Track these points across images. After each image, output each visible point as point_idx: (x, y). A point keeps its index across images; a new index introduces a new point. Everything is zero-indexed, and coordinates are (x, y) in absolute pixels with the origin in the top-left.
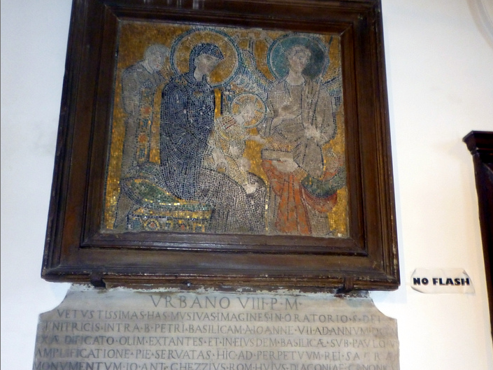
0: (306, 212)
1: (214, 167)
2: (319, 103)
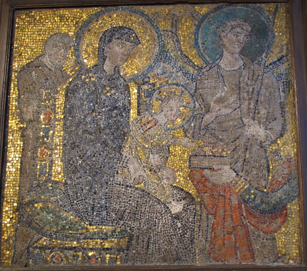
0: (247, 233)
1: (130, 182)
2: (263, 91)
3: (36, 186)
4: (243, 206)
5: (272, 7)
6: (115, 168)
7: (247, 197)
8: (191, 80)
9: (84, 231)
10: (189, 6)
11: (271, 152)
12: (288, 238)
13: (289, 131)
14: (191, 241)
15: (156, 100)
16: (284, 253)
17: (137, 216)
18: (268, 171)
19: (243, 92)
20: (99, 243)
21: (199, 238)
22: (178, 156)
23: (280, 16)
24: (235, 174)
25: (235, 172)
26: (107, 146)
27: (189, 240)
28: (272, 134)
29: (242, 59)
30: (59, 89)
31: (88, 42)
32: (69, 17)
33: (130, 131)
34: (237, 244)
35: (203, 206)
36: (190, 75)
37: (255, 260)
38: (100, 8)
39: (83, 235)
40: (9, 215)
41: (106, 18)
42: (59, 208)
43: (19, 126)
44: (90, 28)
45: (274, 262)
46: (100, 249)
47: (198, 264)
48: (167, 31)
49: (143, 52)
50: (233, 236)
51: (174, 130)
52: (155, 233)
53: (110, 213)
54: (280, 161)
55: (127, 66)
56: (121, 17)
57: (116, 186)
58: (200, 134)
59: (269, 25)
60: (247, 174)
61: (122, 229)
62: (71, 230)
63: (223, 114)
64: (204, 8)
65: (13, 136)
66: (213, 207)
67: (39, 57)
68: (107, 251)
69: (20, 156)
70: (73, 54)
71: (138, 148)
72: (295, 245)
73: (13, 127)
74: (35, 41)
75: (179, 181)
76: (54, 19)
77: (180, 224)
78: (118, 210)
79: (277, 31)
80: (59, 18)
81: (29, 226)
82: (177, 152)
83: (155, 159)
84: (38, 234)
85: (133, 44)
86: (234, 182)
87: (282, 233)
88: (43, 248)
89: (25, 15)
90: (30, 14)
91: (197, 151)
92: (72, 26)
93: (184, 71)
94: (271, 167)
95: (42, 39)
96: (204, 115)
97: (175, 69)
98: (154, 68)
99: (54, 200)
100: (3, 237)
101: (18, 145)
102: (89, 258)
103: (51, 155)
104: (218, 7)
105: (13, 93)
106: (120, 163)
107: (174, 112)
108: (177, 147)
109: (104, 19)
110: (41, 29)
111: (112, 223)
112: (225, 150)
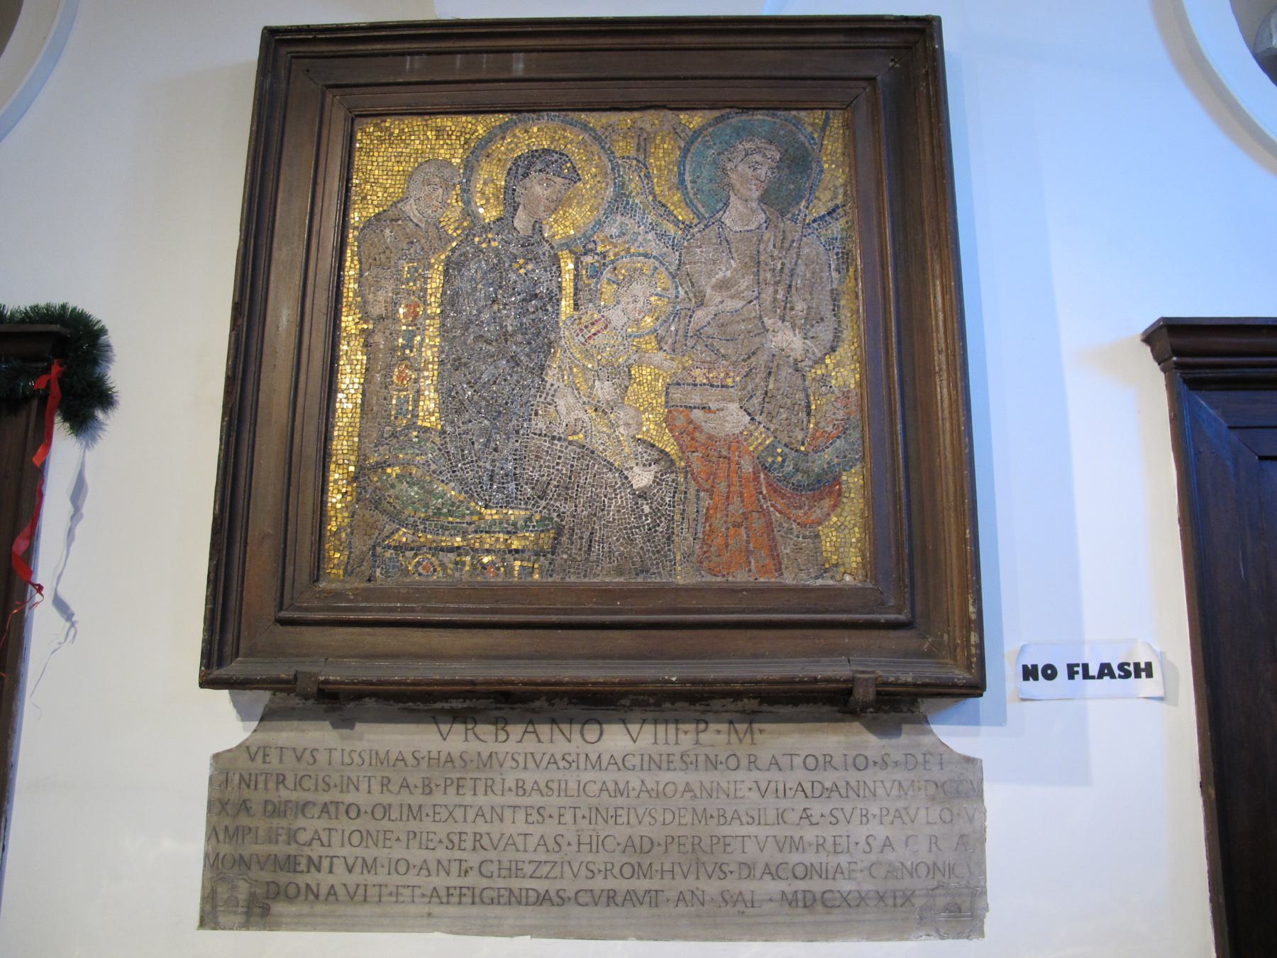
0: (769, 525)
1: (559, 431)
2: (801, 269)
3: (390, 436)
4: (762, 476)
5: (819, 116)
6: (532, 405)
7: (770, 460)
8: (670, 248)
9: (475, 518)
10: (670, 114)
11: (813, 379)
12: (842, 536)
13: (846, 342)
14: (668, 539)
15: (608, 283)
16: (834, 562)
17: (570, 492)
18: (809, 414)
19: (765, 271)
20: (502, 540)
21: (682, 533)
22: (646, 385)
23: (832, 134)
24: (748, 418)
25: (749, 414)
26: (518, 365)
27: (663, 537)
28: (816, 346)
29: (763, 210)
30: (433, 261)
31: (486, 176)
32: (453, 131)
33: (560, 338)
34: (751, 545)
35: (689, 476)
36: (669, 239)
37: (782, 574)
38: (509, 115)
39: (473, 525)
40: (340, 487)
41: (518, 134)
42: (430, 475)
43: (360, 327)
44: (490, 151)
45: (817, 578)
46: (504, 551)
47: (680, 580)
48: (628, 158)
49: (586, 197)
50: (743, 530)
51: (640, 337)
52: (602, 522)
53: (522, 487)
54: (829, 395)
55: (556, 221)
56: (546, 133)
57: (533, 438)
58: (686, 345)
59: (813, 149)
60: (770, 419)
61: (543, 514)
62: (452, 516)
63: (728, 309)
64: (696, 118)
65: (348, 344)
67: (399, 202)
68: (516, 555)
69: (362, 380)
70: (459, 198)
71: (575, 370)
72: (855, 548)
73: (349, 329)
74: (390, 173)
75: (648, 430)
76: (426, 134)
77: (648, 507)
78: (537, 481)
79: (828, 160)
80: (434, 133)
81: (376, 508)
82: (645, 377)
83: (604, 390)
84: (391, 523)
85: (567, 181)
86: (745, 433)
87: (832, 526)
88: (401, 547)
89: (374, 127)
90: (383, 125)
91: (681, 376)
92: (458, 147)
93: (658, 232)
94: (813, 407)
95: (403, 171)
96: (694, 312)
97: (642, 227)
98: (605, 225)
99: (421, 462)
100: (329, 527)
101: (357, 360)
102: (484, 567)
103: (416, 381)
104: (722, 116)
105: (350, 267)
106: (540, 396)
107: (639, 305)
108: (644, 368)
109: (515, 136)
110: (402, 152)
111: (526, 503)
112: (732, 374)
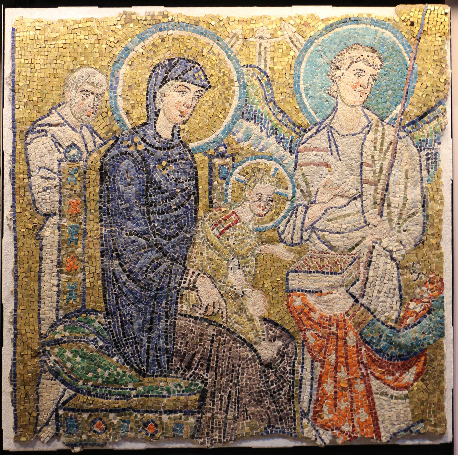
66: (321, 350)
111: (176, 372)
